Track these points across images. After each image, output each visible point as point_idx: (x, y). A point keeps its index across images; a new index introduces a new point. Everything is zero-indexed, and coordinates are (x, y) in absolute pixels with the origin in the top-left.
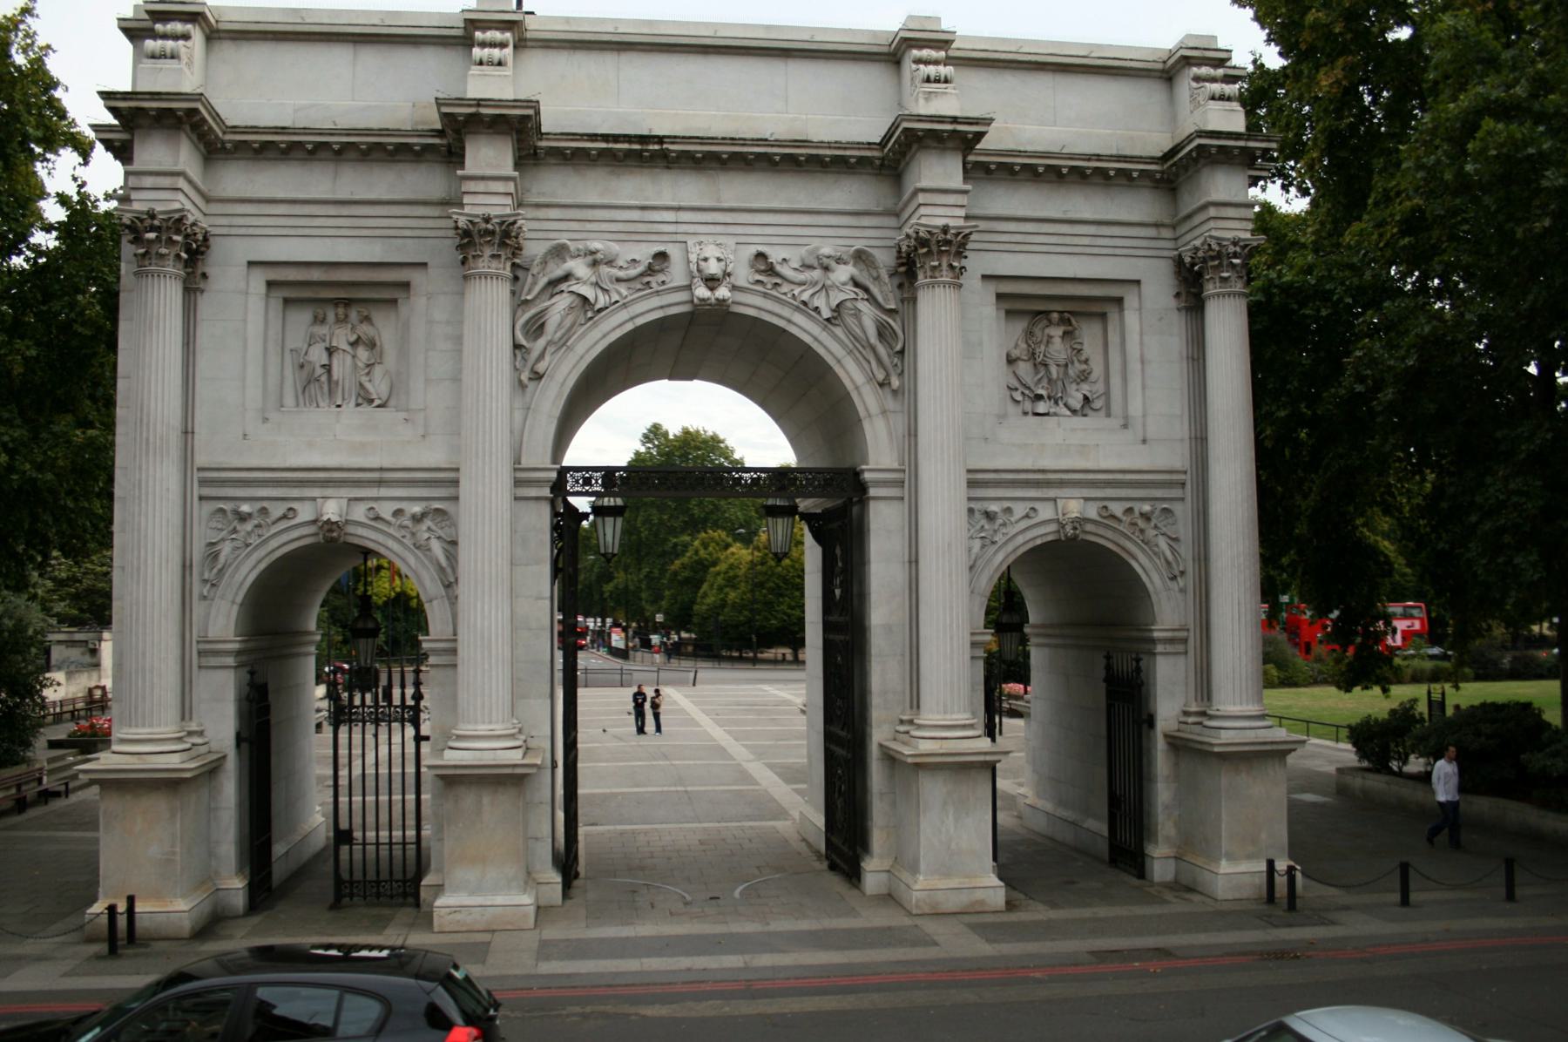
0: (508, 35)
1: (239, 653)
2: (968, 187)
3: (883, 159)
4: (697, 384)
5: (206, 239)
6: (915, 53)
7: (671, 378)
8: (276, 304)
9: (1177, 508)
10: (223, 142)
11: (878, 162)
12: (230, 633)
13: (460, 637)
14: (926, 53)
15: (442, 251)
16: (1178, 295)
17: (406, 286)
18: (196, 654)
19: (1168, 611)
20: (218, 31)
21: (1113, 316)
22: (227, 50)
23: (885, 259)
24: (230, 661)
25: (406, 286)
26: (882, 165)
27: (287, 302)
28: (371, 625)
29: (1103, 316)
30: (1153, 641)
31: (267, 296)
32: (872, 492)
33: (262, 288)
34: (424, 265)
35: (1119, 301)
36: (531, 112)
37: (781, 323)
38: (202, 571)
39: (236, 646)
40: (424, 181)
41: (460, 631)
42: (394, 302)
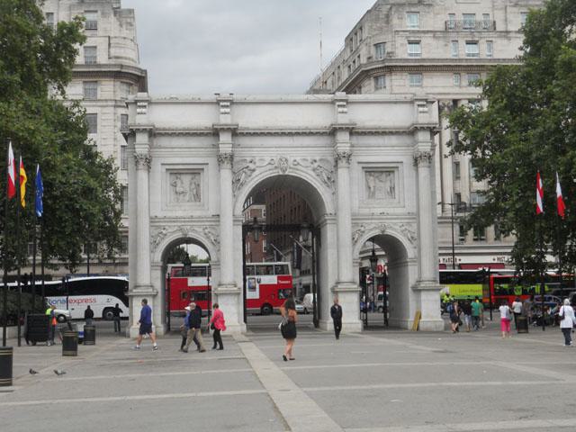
6: (338, 103)
8: (168, 175)
9: (413, 225)
15: (212, 161)
17: (203, 169)
18: (153, 265)
19: (411, 252)
22: (154, 107)
23: (331, 159)
27: (171, 174)
29: (393, 172)
30: (407, 262)
32: (328, 222)
34: (207, 164)
38: (154, 244)
40: (207, 141)
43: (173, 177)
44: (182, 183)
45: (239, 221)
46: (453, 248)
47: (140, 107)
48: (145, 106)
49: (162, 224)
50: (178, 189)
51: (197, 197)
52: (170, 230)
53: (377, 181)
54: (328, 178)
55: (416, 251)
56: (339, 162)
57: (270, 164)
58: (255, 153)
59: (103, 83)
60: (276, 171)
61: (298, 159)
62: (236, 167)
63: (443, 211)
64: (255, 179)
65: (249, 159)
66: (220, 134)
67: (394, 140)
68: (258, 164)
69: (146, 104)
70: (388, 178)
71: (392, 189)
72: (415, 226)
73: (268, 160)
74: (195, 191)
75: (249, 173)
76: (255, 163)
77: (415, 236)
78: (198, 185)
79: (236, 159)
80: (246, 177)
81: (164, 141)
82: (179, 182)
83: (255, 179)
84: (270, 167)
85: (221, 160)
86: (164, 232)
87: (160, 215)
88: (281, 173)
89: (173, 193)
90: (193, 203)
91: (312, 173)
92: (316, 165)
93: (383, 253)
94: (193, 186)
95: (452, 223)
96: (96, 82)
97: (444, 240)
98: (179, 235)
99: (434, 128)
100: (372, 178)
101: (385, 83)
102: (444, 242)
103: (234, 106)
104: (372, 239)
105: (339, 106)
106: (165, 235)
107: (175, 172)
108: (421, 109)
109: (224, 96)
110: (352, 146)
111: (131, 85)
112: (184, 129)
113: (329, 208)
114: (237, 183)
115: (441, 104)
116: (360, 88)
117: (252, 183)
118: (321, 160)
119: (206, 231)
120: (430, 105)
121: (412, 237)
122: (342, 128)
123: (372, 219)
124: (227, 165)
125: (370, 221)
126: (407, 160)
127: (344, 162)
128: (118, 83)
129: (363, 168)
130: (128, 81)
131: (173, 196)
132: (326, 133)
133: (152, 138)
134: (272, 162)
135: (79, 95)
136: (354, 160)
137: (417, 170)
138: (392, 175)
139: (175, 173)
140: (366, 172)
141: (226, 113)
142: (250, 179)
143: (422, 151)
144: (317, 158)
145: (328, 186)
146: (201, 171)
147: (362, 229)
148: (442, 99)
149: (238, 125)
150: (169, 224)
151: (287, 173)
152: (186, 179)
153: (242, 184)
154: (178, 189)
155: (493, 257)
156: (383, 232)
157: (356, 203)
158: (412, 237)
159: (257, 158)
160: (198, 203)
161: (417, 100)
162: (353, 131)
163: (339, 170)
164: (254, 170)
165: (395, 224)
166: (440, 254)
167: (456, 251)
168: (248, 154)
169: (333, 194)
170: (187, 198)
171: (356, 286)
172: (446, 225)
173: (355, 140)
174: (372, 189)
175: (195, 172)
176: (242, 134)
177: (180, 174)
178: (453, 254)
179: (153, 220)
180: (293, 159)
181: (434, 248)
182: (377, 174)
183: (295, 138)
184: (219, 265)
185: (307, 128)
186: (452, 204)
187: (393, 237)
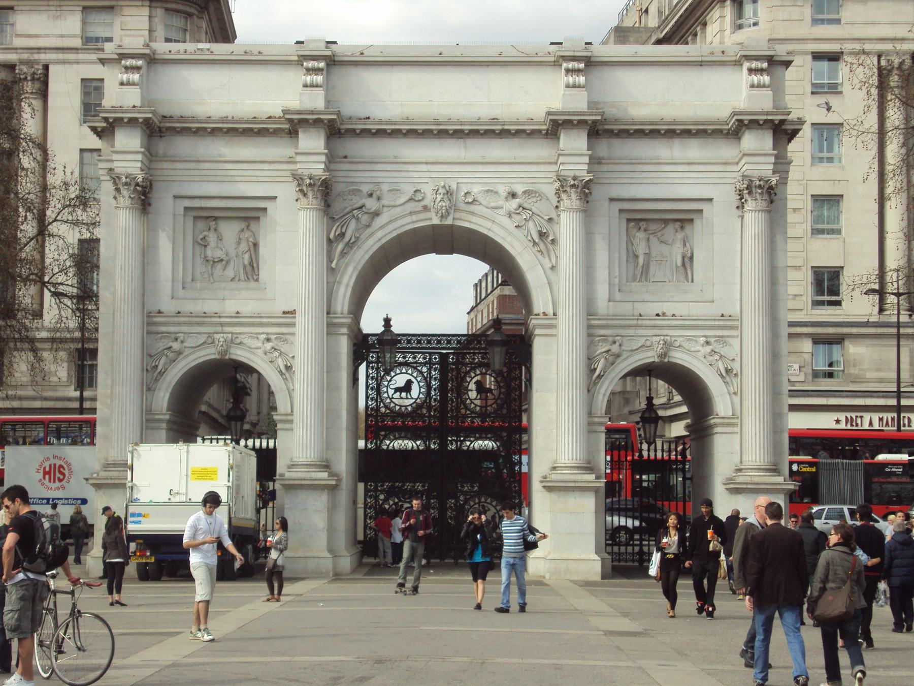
0: (322, 65)
1: (169, 422)
2: (590, 152)
3: (548, 130)
4: (456, 258)
5: (151, 185)
7: (438, 252)
10: (160, 128)
11: (544, 132)
12: (164, 411)
13: (295, 413)
14: (571, 65)
15: (286, 191)
16: (738, 207)
17: (265, 209)
19: (722, 405)
20: (155, 59)
21: (697, 223)
22: (160, 68)
23: (549, 190)
24: (164, 425)
25: (265, 209)
26: (547, 134)
27: (195, 218)
28: (239, 413)
29: (691, 221)
31: (184, 216)
32: (537, 332)
33: (182, 211)
34: (276, 198)
35: (701, 211)
36: (334, 117)
37: (485, 232)
38: (151, 374)
39: (168, 417)
41: (295, 410)
42: (258, 218)
43: (201, 224)
44: (220, 238)
45: (341, 325)
46: (899, 394)
47: (127, 68)
48: (138, 68)
49: (172, 329)
50: (209, 253)
51: (252, 270)
52: (190, 343)
53: (654, 240)
54: (542, 235)
55: (737, 400)
56: (564, 196)
57: (411, 199)
58: (384, 176)
59: (127, 11)
60: (428, 215)
61: (476, 189)
62: (338, 206)
63: (881, 310)
64: (379, 234)
65: (365, 189)
66: (300, 130)
67: (693, 150)
68: (384, 202)
69: (140, 63)
70: (680, 235)
71: (688, 260)
72: (736, 343)
73: (410, 191)
74: (247, 256)
75: (365, 219)
76: (379, 199)
77: (736, 366)
78: (256, 245)
79: (338, 188)
80: (358, 229)
81: (184, 146)
82: (212, 238)
83: (379, 234)
84: (412, 206)
85: (304, 185)
86: (176, 346)
87: (168, 305)
88: (436, 221)
89: (199, 261)
90: (242, 285)
91: (506, 221)
92: (514, 204)
93: (684, 409)
94: (244, 247)
95: (899, 336)
96: (112, 7)
97: (881, 375)
98: (209, 354)
99: (782, 122)
100: (641, 235)
101: (755, 14)
102: (881, 381)
103: (338, 72)
104: (647, 371)
105: (568, 71)
106: (179, 353)
107: (205, 214)
108: (755, 79)
109: (312, 46)
110: (595, 161)
111: (190, 15)
112: (224, 120)
113: (540, 302)
114: (335, 243)
115: (883, 63)
116: (705, 25)
117: (371, 242)
118: (525, 192)
119: (269, 346)
120: (779, 70)
121: (728, 371)
122: (570, 121)
123: (637, 327)
124: (312, 201)
125: (631, 332)
126: (723, 194)
127: (574, 196)
128: (160, 12)
129: (621, 211)
130: (181, 7)
131: (200, 268)
132: (540, 131)
133: (156, 140)
134: (419, 196)
135: (75, 36)
136: (600, 193)
137: (742, 217)
138: (688, 227)
139: (205, 217)
140: (629, 220)
141: (312, 86)
142: (369, 231)
143: (756, 174)
144: (519, 189)
145: (540, 251)
146: (260, 214)
147: (615, 349)
148: (888, 53)
149: (338, 113)
150: (185, 329)
151: (449, 221)
152: (230, 230)
153: (350, 245)
154: (209, 253)
155: (835, 416)
156: (664, 355)
157: (602, 291)
158: (728, 371)
159: (385, 188)
160: (252, 284)
161: (748, 58)
162: (599, 130)
163: (563, 216)
164: (376, 214)
165: (690, 339)
166: (794, 408)
167: (904, 402)
168: (363, 177)
169: (553, 268)
170: (230, 272)
171: (592, 477)
172: (886, 342)
173: (604, 147)
174: (641, 261)
175: (250, 215)
176: (353, 133)
177: (216, 219)
178: (899, 409)
179: (151, 322)
180: (464, 189)
181: (774, 392)
182: (653, 227)
183: (470, 142)
184: (291, 421)
185: (494, 120)
186: (898, 295)
187: (689, 370)
